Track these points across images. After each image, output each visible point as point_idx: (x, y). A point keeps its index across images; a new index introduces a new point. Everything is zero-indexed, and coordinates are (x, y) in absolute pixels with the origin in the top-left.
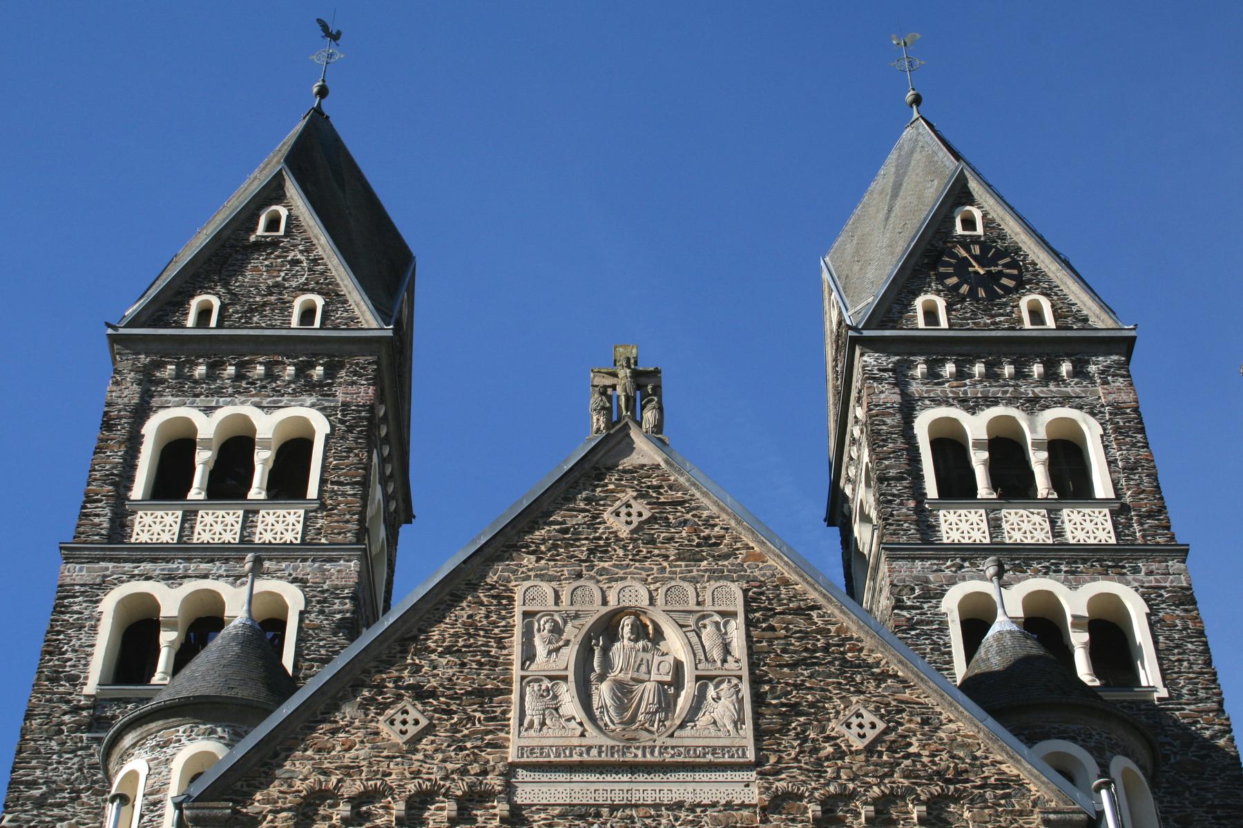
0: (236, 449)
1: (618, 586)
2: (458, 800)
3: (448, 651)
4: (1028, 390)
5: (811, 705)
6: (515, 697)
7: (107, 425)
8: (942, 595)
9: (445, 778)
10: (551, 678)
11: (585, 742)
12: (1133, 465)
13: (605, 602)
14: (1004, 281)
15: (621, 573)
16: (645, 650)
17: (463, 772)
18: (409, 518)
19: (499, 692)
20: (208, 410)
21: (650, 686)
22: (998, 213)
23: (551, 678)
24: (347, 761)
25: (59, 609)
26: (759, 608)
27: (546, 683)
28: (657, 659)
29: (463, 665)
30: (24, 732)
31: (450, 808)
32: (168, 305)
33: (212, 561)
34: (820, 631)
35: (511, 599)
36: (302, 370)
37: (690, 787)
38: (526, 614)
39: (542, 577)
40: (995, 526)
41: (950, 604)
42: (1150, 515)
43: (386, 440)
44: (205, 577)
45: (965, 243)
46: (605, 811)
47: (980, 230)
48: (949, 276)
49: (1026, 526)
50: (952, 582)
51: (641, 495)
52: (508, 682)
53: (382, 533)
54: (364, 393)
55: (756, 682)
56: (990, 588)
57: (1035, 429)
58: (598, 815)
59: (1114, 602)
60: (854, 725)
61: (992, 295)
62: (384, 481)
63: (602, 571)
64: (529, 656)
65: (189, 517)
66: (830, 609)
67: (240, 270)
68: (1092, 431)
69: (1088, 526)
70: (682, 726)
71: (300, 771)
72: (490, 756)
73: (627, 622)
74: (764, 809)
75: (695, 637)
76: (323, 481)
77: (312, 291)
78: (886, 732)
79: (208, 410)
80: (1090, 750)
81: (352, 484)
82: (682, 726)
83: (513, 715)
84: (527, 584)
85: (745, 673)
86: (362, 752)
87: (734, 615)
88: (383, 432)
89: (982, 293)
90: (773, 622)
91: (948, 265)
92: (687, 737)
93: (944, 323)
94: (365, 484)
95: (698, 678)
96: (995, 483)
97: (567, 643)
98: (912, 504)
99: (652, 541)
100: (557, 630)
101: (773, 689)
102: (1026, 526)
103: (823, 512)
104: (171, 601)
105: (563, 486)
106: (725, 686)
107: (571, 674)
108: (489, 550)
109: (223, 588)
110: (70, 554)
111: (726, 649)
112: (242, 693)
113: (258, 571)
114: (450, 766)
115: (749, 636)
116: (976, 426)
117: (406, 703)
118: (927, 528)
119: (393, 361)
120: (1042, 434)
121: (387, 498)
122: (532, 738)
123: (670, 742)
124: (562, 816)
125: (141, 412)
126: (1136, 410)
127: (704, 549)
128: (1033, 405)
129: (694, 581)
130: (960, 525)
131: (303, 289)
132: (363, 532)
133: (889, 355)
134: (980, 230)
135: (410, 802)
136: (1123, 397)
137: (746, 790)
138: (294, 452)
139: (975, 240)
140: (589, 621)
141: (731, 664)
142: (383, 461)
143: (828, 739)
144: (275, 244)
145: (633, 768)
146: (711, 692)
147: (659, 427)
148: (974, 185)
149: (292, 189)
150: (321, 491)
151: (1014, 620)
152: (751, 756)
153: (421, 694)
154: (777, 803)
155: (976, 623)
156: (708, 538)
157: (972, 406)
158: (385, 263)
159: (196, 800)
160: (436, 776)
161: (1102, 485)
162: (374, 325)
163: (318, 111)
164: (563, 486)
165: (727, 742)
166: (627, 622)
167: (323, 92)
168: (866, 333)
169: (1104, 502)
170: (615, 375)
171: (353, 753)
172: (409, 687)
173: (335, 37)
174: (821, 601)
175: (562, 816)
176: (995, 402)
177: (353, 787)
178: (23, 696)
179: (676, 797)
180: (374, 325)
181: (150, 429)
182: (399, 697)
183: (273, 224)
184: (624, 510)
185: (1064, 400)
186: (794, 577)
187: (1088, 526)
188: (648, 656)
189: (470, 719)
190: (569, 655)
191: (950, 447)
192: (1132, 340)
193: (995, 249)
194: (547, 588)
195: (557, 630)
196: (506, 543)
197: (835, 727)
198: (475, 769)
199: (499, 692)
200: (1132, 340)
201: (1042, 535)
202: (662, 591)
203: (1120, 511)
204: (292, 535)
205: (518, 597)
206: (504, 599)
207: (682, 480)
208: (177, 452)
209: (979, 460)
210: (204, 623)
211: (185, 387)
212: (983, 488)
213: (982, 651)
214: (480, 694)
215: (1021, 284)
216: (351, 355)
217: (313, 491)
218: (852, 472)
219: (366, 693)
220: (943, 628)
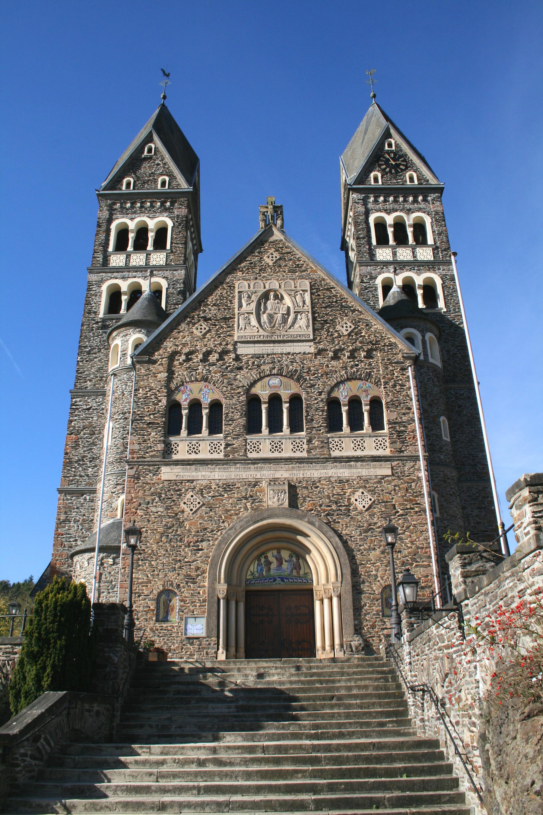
0: (142, 231)
1: (269, 282)
2: (219, 353)
3: (214, 305)
4: (407, 206)
5: (331, 320)
6: (236, 320)
7: (99, 226)
8: (376, 278)
9: (215, 346)
10: (248, 313)
11: (259, 334)
12: (441, 234)
13: (265, 288)
14: (401, 167)
15: (270, 277)
16: (278, 303)
17: (220, 344)
18: (201, 251)
19: (231, 318)
20: (132, 219)
21: (280, 315)
22: (400, 141)
23: (248, 313)
24: (183, 342)
25: (89, 290)
26: (314, 288)
27: (246, 315)
28: (282, 306)
29: (219, 309)
30: (81, 330)
31: (217, 356)
32: (116, 182)
33: (137, 272)
34: (334, 296)
35: (234, 287)
36: (163, 204)
37: (292, 348)
38: (239, 292)
39: (244, 279)
40: (394, 254)
41: (379, 281)
42: (445, 250)
43: (192, 226)
44: (135, 277)
45: (389, 153)
46: (265, 356)
47: (394, 148)
48: (383, 165)
49: (404, 254)
50: (380, 273)
51: (276, 251)
52: (234, 315)
53: (193, 258)
54: (184, 211)
55: (313, 313)
56: (391, 275)
57: (409, 220)
58: (263, 357)
59: (431, 279)
60: (344, 327)
61: (397, 172)
62: (192, 240)
63: (264, 277)
64: (240, 306)
65: (128, 257)
66: (338, 288)
67: (139, 168)
68: (428, 221)
69: (425, 254)
70: (290, 328)
71: (169, 345)
72: (229, 339)
73: (272, 294)
74: (315, 354)
75: (294, 298)
76: (172, 243)
77: (164, 175)
78: (354, 329)
79: (132, 219)
80: (419, 331)
81: (181, 244)
82: (290, 328)
83: (236, 326)
84: (239, 282)
85: (310, 310)
86: (188, 339)
87: (306, 291)
88: (191, 224)
89: (393, 171)
90: (319, 293)
91: (382, 161)
92: (292, 332)
93: (380, 183)
94: (186, 243)
95: (295, 312)
96: (395, 239)
97: (253, 301)
98: (367, 247)
99: (280, 266)
100: (249, 297)
101: (319, 315)
102: (404, 254)
103: (339, 246)
104: (124, 286)
105: (251, 247)
106: (303, 315)
107: (254, 312)
108: (227, 271)
109: (140, 281)
110: (91, 271)
111: (304, 303)
112: (149, 318)
113: (152, 275)
114: (216, 343)
115: (311, 298)
116: (390, 219)
117: (201, 322)
118: (372, 255)
119: (193, 200)
120: (411, 222)
121: (193, 245)
122: (242, 333)
123: (286, 333)
124: (252, 358)
125: (110, 221)
126: (443, 213)
127: (297, 269)
128: (409, 211)
129: (294, 279)
130: (383, 254)
131: (161, 174)
132: (186, 260)
133: (361, 194)
134: (394, 148)
135: (204, 355)
136: (439, 209)
137: (310, 348)
138: (161, 232)
139: (392, 152)
140: (260, 294)
141: (306, 307)
142: (191, 233)
143: (336, 331)
144: (151, 158)
145: (274, 342)
146: (299, 317)
147: (282, 226)
148: (392, 131)
149: (156, 137)
150: (171, 247)
151: (399, 287)
152: (311, 337)
153: (206, 319)
154: (320, 352)
155: (387, 288)
156: (298, 265)
158: (188, 162)
159: (138, 355)
160: (212, 346)
161: (430, 240)
162: (186, 187)
163: (163, 105)
164: (251, 247)
165: (304, 333)
166: (272, 294)
167: (165, 97)
168: (354, 186)
169: (431, 246)
170: (267, 208)
171: (185, 339)
172: (202, 317)
173: (168, 75)
174: (335, 286)
175: (252, 358)
176: (396, 211)
177: (186, 350)
178: (80, 319)
179: (288, 351)
180: (186, 187)
181: (113, 226)
182: (199, 321)
183: (150, 150)
184: (271, 256)
185: (419, 210)
186: (326, 278)
187: (425, 254)
188: (279, 305)
189: (222, 327)
190: (253, 305)
191: (381, 226)
192: (442, 189)
193: (399, 155)
194: (246, 283)
195: (249, 297)
196: (232, 268)
197: (338, 327)
198: (224, 343)
199: (231, 318)
200: (442, 189)
201: (410, 258)
202: (283, 283)
203: (435, 249)
204: (162, 262)
205: (236, 286)
206: (232, 287)
207: (290, 245)
208: (123, 233)
209: (390, 231)
210: (135, 293)
211: (124, 211)
212: (391, 242)
213: (388, 297)
214: (225, 319)
215: (407, 168)
216: (179, 198)
217: (168, 247)
218: (349, 233)
219: (189, 320)
220: (376, 289)
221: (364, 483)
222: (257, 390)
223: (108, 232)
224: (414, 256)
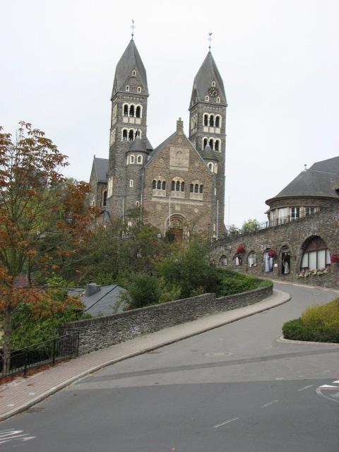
41: (203, 139)
49: (212, 130)
60: (197, 165)
69: (218, 131)
116: (209, 116)
125: (122, 103)
128: (216, 114)
130: (206, 129)
144: (134, 77)
154: (190, 171)
157: (209, 113)
187: (218, 131)
211: (127, 101)
221: (197, 207)
222: (174, 179)
223: (121, 108)
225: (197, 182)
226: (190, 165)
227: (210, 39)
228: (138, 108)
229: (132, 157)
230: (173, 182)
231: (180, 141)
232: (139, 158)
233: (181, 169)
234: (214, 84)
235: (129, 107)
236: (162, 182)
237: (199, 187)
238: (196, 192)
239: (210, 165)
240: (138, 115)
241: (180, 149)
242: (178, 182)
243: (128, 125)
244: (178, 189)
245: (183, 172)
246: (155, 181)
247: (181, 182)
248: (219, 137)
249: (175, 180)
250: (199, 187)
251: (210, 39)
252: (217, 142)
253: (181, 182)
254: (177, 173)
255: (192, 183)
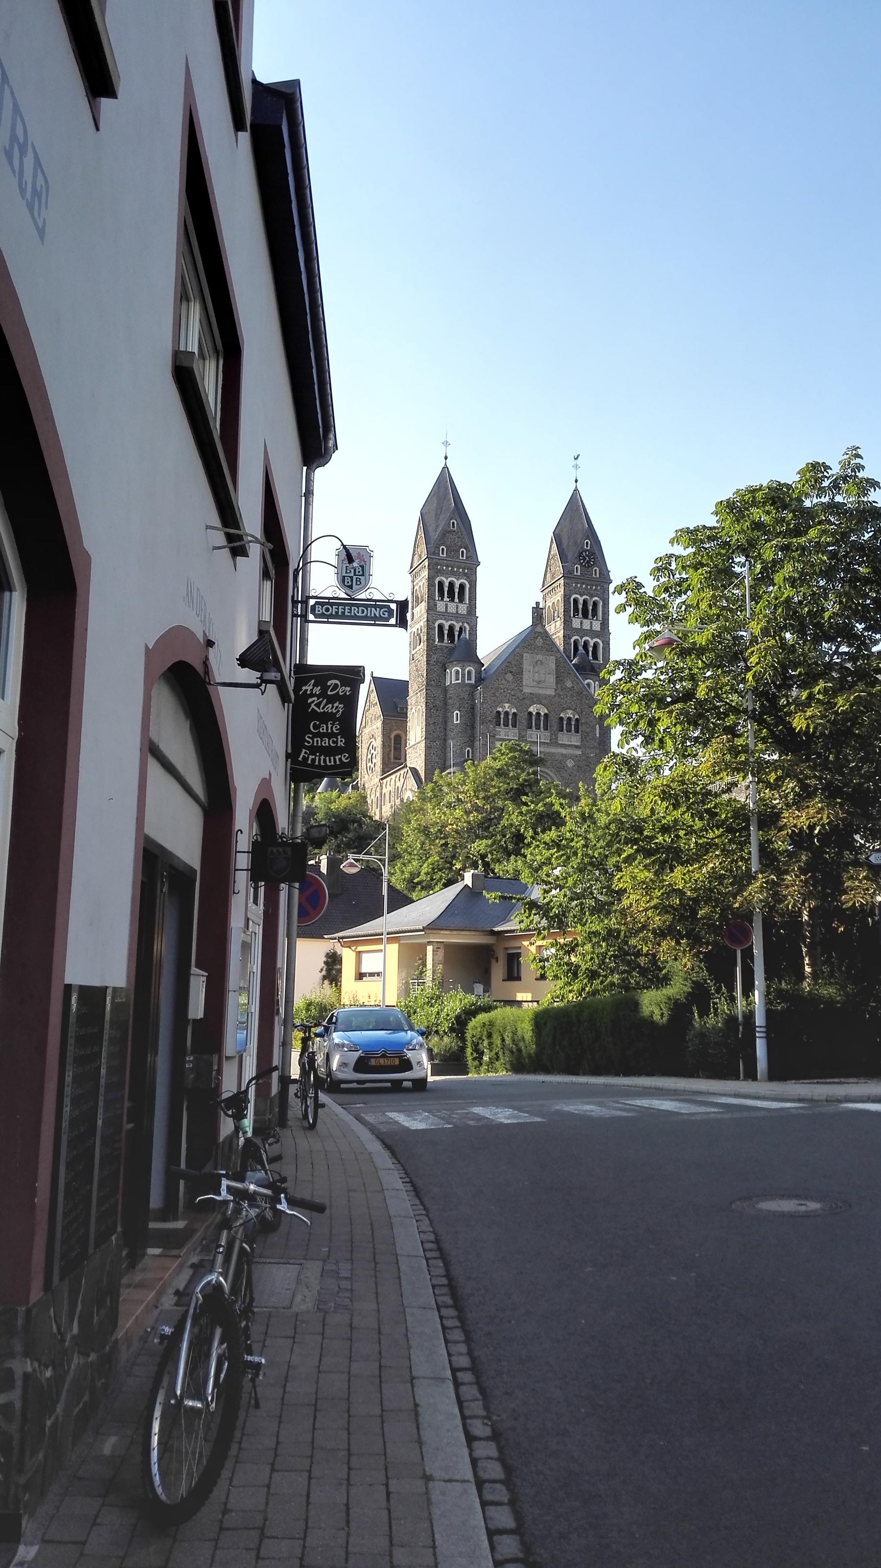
36: (464, 571)
41: (572, 640)
60: (569, 684)
116: (581, 600)
128: (592, 596)
221: (571, 757)
222: (531, 709)
224: (591, 627)
225: (570, 714)
226: (557, 683)
227: (576, 467)
228: (462, 587)
229: (457, 672)
230: (530, 714)
231: (539, 642)
232: (469, 673)
233: (541, 692)
234: (587, 544)
235: (447, 584)
236: (511, 713)
237: (573, 723)
238: (569, 731)
239: (588, 685)
240: (461, 600)
241: (540, 657)
242: (538, 714)
243: (446, 615)
244: (538, 727)
245: (546, 697)
246: (499, 713)
247: (542, 714)
248: (597, 637)
249: (533, 709)
250: (573, 723)
251: (576, 467)
252: (595, 646)
253: (542, 714)
254: (536, 699)
255: (562, 715)
